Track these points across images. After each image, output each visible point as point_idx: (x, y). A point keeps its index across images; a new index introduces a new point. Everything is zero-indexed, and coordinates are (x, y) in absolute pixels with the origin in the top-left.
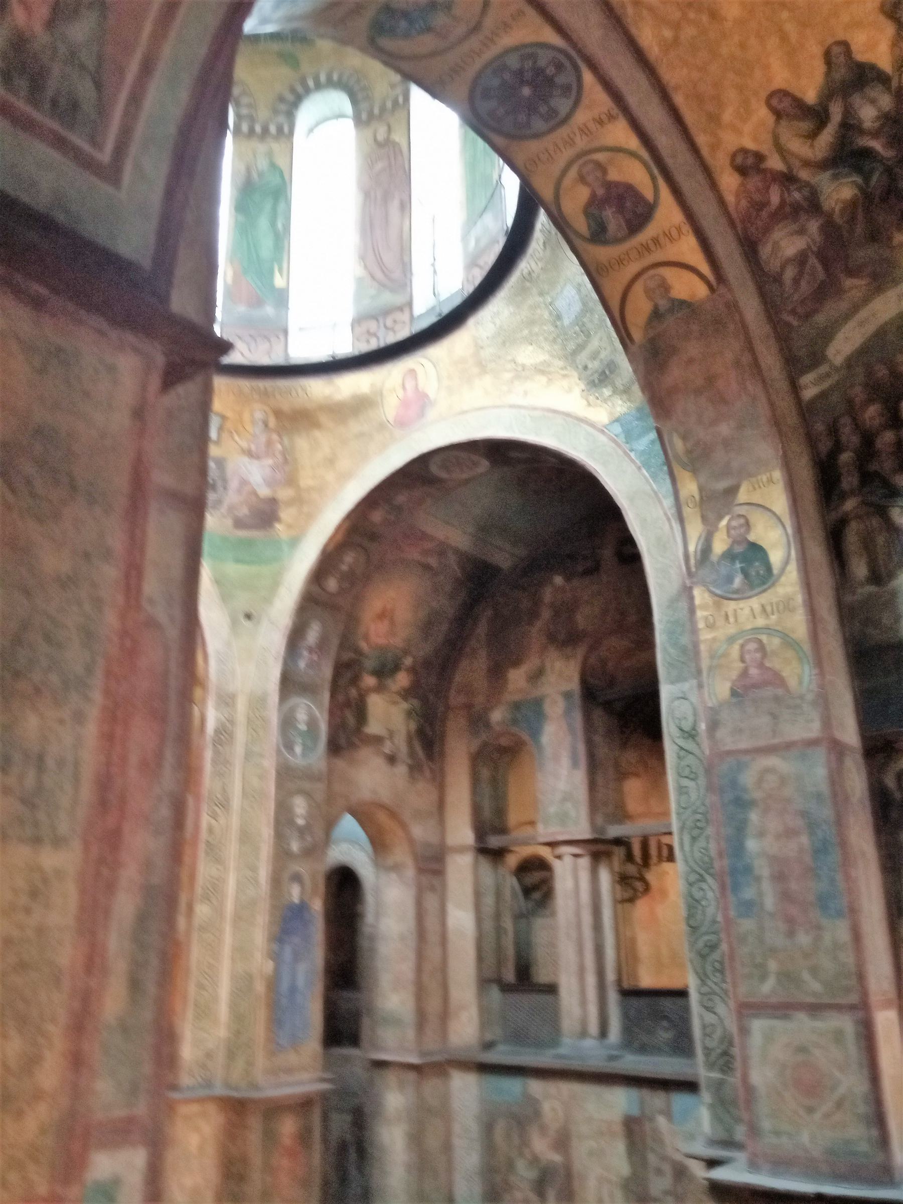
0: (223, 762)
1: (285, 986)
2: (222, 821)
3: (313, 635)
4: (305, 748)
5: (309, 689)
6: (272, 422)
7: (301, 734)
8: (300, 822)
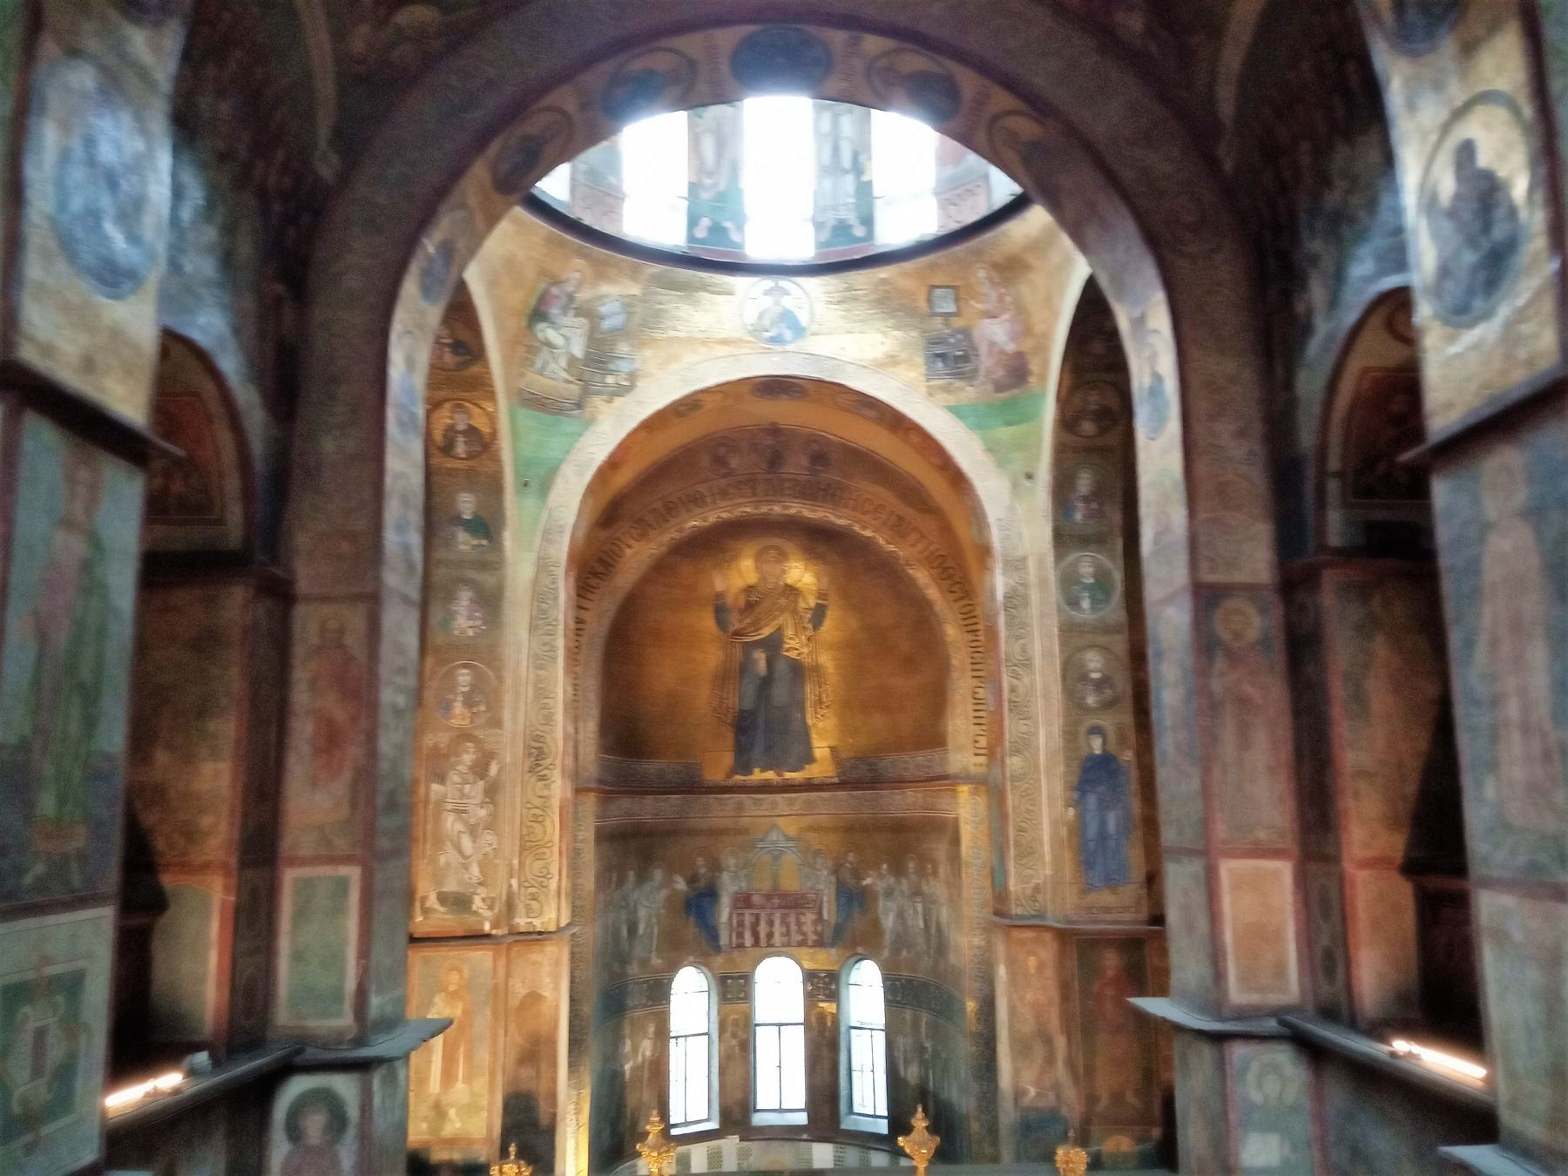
0: (1019, 628)
1: (1092, 831)
2: (1026, 680)
3: (1084, 483)
4: (1094, 601)
5: (1085, 541)
6: (996, 276)
7: (1087, 587)
8: (1095, 676)
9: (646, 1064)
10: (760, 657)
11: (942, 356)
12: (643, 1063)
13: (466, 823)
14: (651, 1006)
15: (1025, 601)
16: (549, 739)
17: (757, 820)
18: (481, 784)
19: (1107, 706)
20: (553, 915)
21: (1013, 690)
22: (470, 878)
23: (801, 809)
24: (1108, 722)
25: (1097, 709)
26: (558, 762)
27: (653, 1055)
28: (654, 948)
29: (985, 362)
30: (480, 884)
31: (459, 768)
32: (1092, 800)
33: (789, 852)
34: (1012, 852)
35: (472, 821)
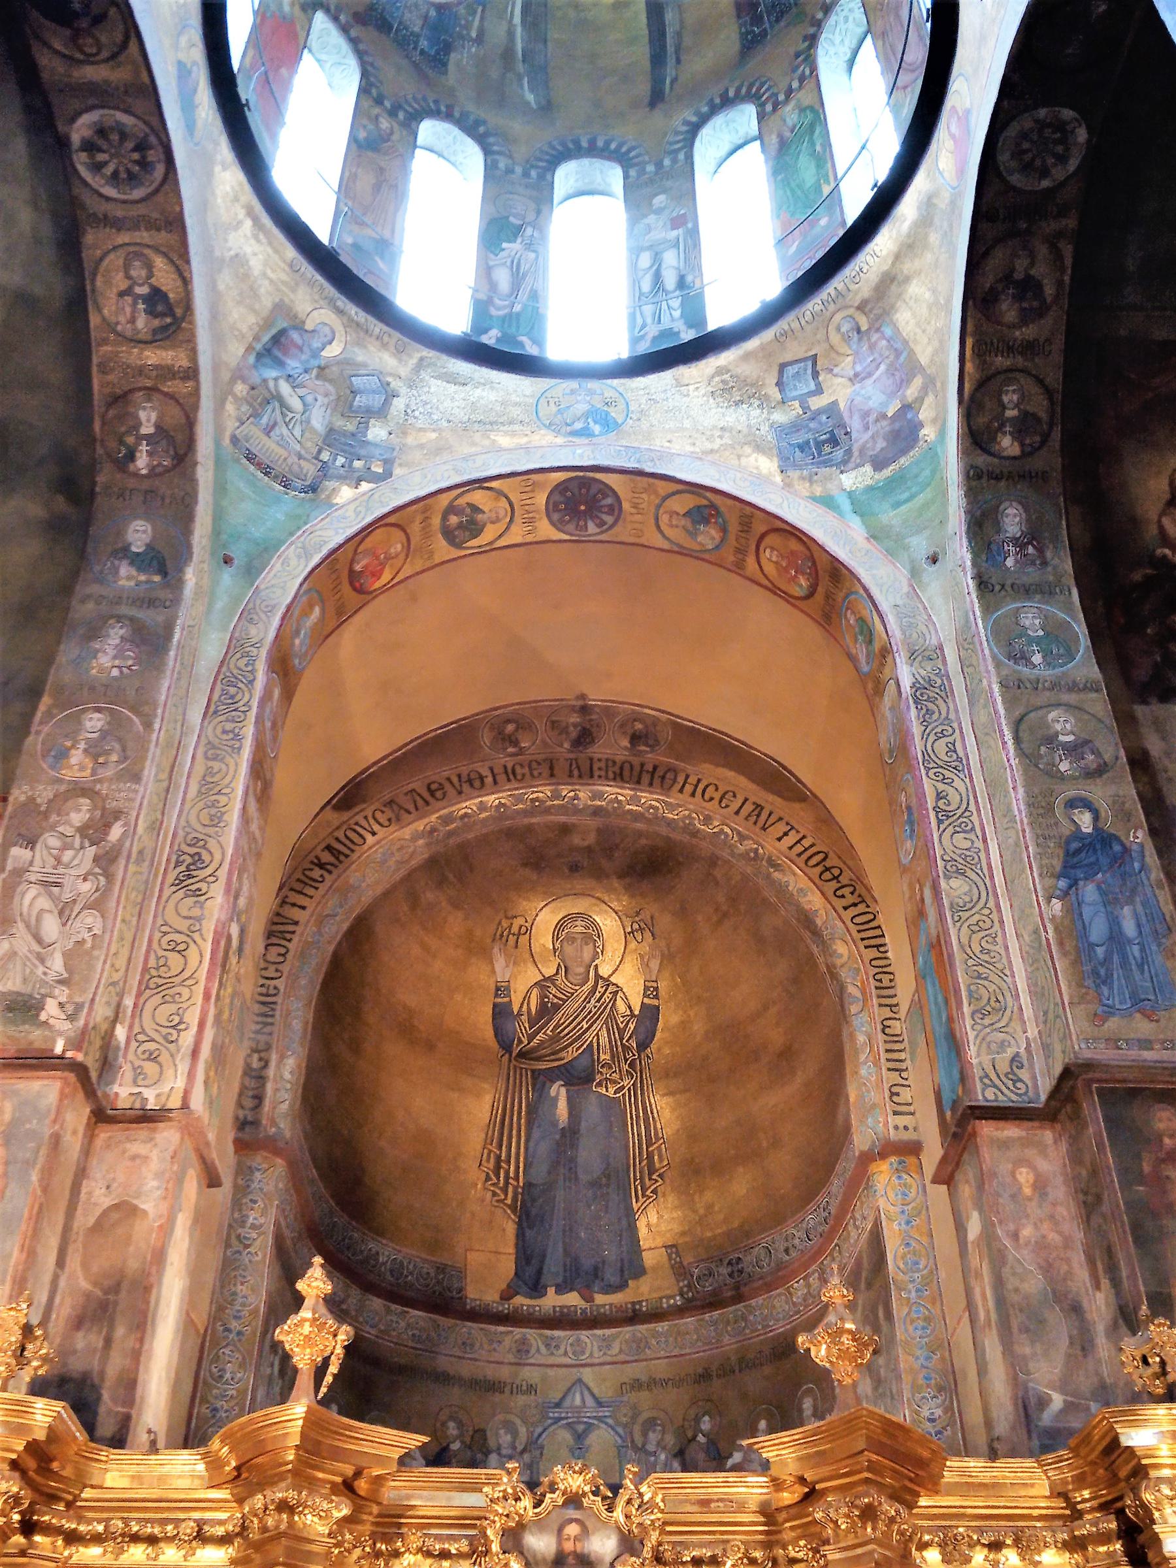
2: (958, 783)
10: (559, 1092)
11: (803, 447)
15: (946, 693)
16: (212, 844)
17: (551, 1372)
18: (91, 851)
20: (180, 1083)
21: (939, 796)
23: (621, 1351)
24: (1099, 793)
26: (223, 874)
29: (860, 437)
31: (60, 829)
32: (1089, 891)
33: (603, 1425)
35: (67, 896)
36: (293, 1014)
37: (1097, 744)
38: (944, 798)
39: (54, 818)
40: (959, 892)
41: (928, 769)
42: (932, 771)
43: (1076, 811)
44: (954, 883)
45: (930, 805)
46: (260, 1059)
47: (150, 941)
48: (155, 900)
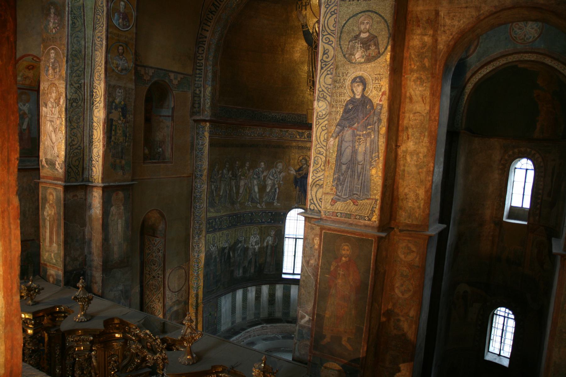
8: (363, 35)
9: (269, 247)
12: (267, 246)
13: (53, 127)
14: (273, 223)
19: (369, 59)
21: (324, 54)
22: (54, 153)
25: (361, 63)
27: (273, 244)
28: (276, 199)
30: (58, 156)
32: (348, 133)
34: (311, 169)
35: (55, 126)
36: (209, 71)
37: (380, 39)
38: (326, 53)
39: (49, 96)
40: (321, 109)
41: (323, 35)
42: (325, 37)
43: (356, 85)
44: (321, 104)
45: (319, 59)
46: (199, 90)
47: (89, 125)
48: (89, 110)
